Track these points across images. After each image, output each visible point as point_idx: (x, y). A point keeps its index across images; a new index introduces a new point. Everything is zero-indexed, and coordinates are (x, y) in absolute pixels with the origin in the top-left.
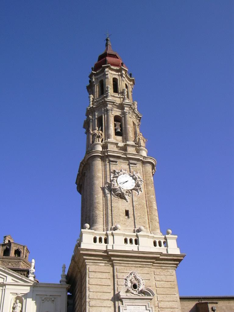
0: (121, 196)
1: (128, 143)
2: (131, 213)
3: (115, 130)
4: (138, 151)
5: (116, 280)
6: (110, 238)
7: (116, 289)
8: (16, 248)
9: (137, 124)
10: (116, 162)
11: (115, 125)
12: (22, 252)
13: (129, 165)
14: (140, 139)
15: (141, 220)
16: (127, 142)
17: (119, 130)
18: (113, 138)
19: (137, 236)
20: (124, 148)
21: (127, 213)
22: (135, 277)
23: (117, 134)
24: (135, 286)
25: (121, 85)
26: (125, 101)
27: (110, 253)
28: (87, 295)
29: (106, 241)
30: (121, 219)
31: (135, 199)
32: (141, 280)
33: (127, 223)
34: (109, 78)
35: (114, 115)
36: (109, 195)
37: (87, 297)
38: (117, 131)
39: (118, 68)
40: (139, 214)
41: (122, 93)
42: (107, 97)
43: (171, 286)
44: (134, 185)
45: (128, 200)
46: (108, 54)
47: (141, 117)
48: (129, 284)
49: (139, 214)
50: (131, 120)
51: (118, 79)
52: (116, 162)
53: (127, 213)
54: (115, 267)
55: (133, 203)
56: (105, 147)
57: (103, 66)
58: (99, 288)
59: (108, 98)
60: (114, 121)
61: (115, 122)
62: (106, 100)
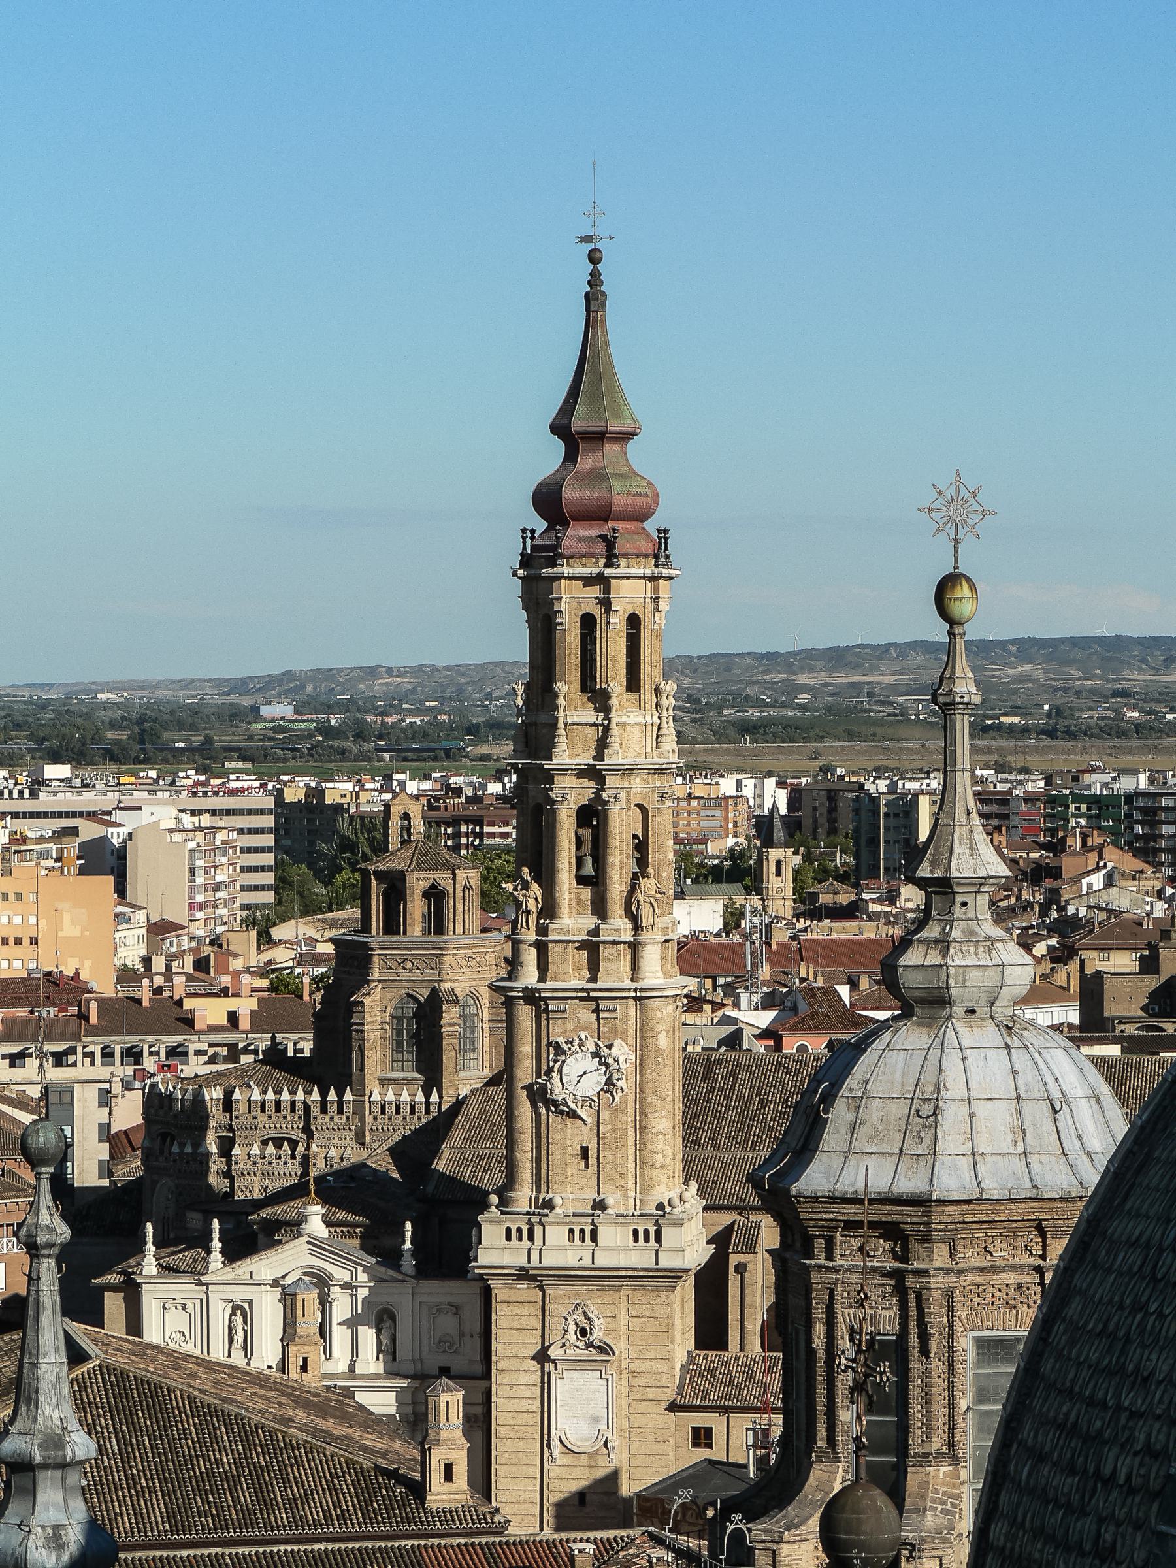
0: (573, 1115)
2: (592, 1153)
5: (546, 1319)
6: (538, 1230)
7: (546, 1337)
8: (425, 885)
10: (564, 1011)
11: (579, 842)
12: (451, 891)
13: (597, 1011)
14: (641, 902)
15: (613, 1172)
19: (593, 1223)
21: (585, 1152)
22: (587, 1317)
24: (583, 1333)
25: (604, 650)
27: (531, 1272)
28: (493, 1349)
29: (531, 1238)
30: (569, 1171)
31: (605, 1115)
32: (595, 1319)
33: (583, 1182)
36: (543, 1111)
37: (493, 1353)
40: (610, 1158)
43: (658, 1328)
44: (603, 1079)
45: (588, 1120)
48: (572, 1328)
49: (610, 1158)
51: (599, 621)
52: (564, 1011)
53: (585, 1152)
54: (547, 1292)
55: (598, 1127)
58: (517, 1337)
60: (579, 826)
61: (580, 831)
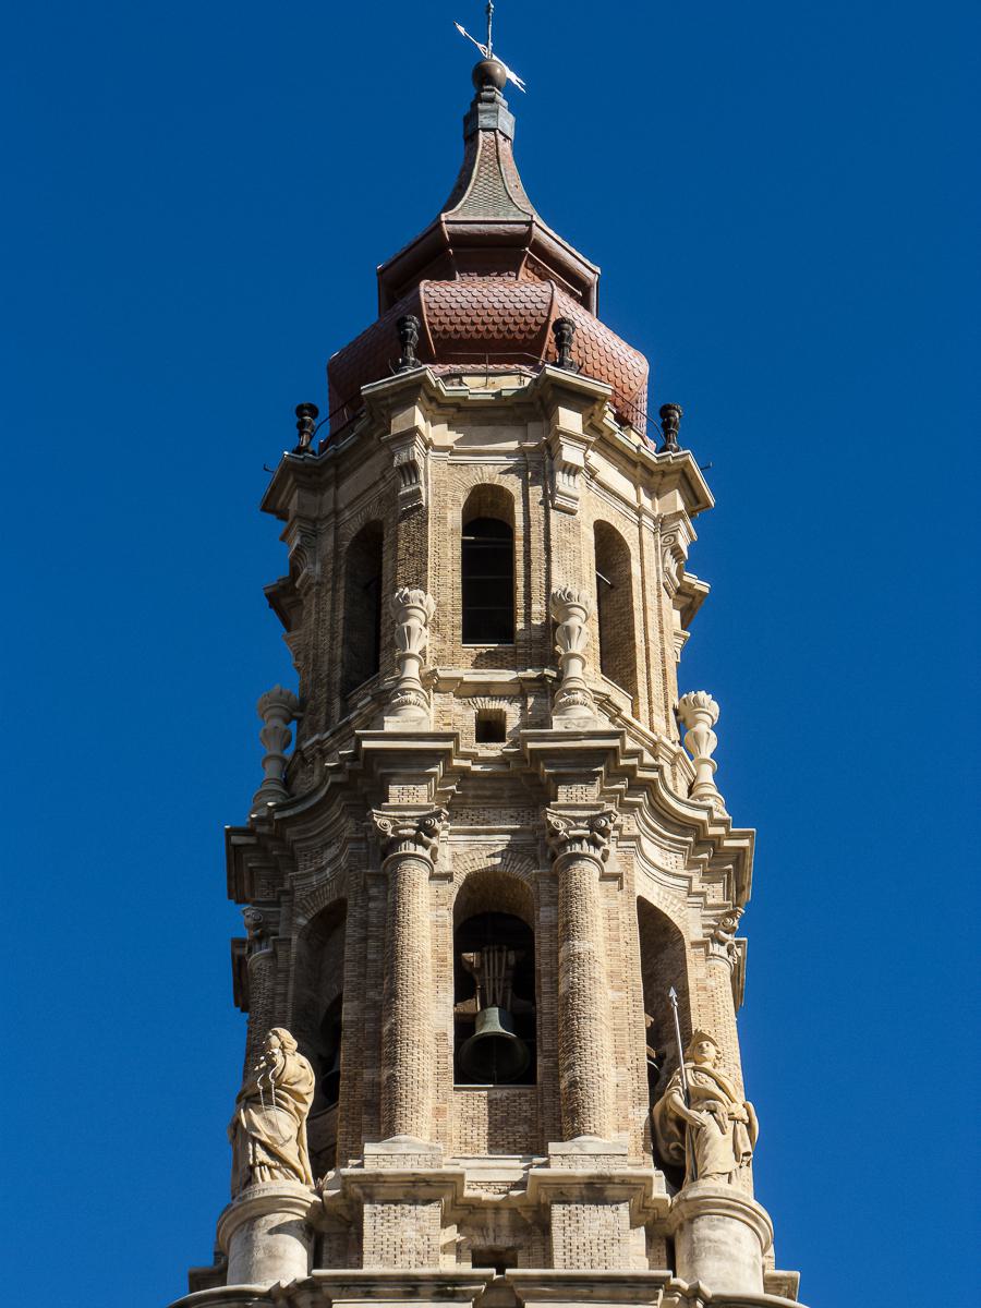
1: (569, 1160)
3: (464, 1026)
4: (667, 1240)
9: (691, 924)
16: (553, 1147)
17: (493, 1024)
18: (439, 1124)
20: (530, 1222)
23: (475, 1061)
26: (558, 726)
34: (428, 497)
35: (459, 879)
38: (480, 1032)
39: (509, 384)
41: (546, 647)
42: (386, 702)
46: (460, 240)
47: (745, 843)
50: (627, 883)
56: (332, 1233)
57: (366, 389)
59: (391, 725)
62: (366, 744)
